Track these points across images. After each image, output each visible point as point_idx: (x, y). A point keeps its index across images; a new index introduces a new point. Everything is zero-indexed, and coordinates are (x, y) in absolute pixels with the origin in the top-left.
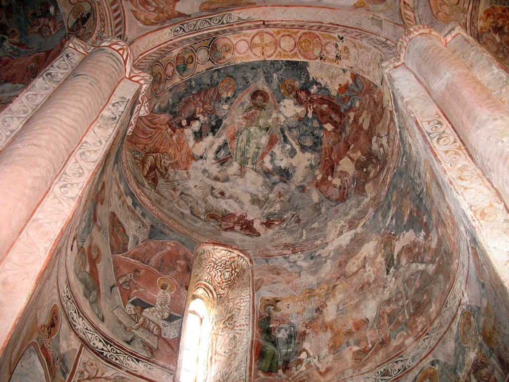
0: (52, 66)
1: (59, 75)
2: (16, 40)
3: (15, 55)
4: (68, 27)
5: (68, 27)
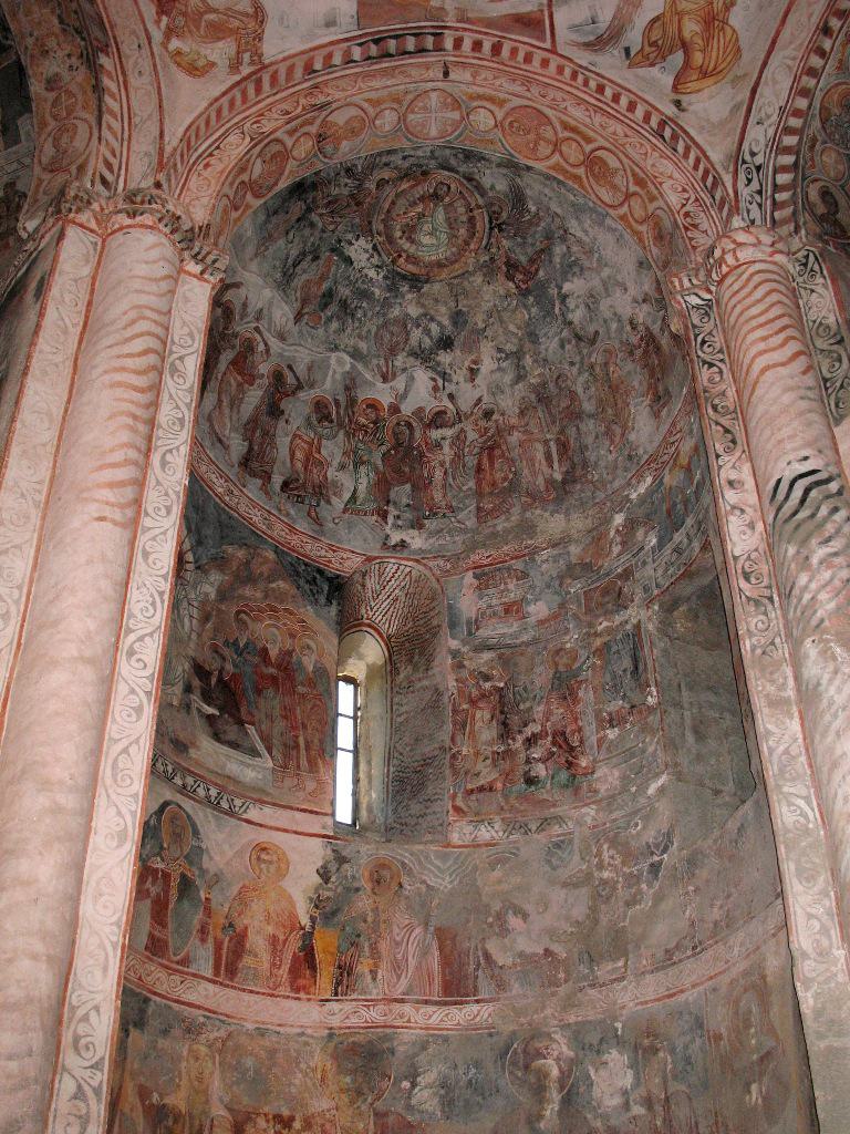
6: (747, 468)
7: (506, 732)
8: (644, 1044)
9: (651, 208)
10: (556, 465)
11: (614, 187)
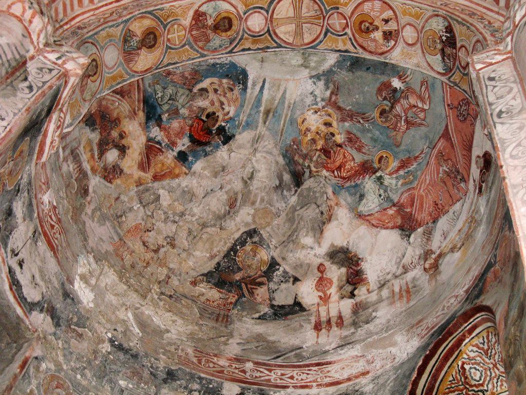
0: (490, 104)
1: (512, 102)
2: (394, 164)
3: (411, 182)
4: (439, 73)
5: (439, 73)
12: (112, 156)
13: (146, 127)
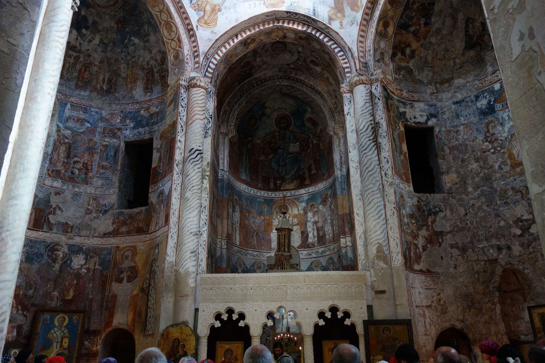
6: (184, 138)
7: (68, 157)
8: (89, 253)
9: (178, 48)
10: (105, 84)
11: (170, 35)
12: (408, 51)
13: (408, 32)
